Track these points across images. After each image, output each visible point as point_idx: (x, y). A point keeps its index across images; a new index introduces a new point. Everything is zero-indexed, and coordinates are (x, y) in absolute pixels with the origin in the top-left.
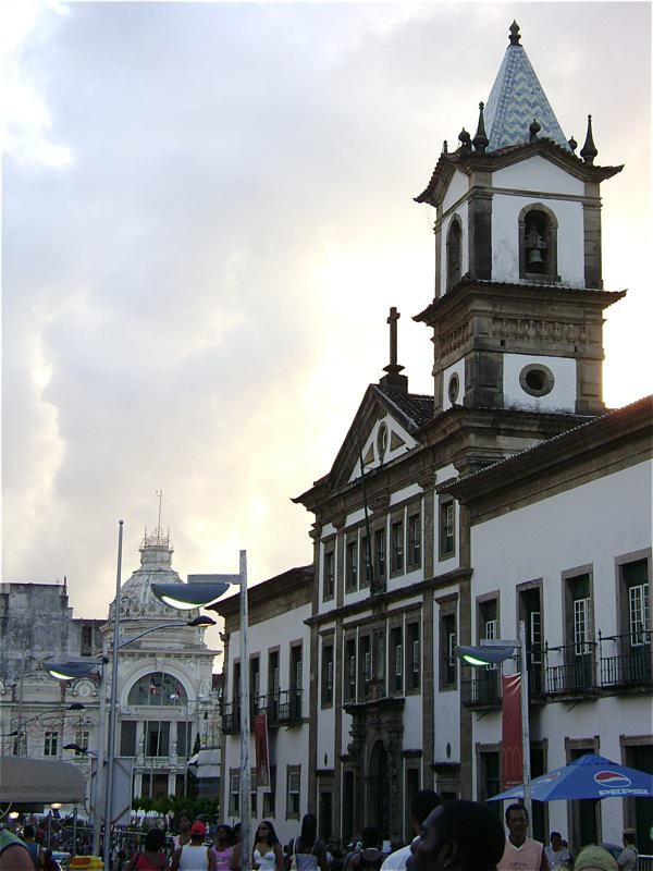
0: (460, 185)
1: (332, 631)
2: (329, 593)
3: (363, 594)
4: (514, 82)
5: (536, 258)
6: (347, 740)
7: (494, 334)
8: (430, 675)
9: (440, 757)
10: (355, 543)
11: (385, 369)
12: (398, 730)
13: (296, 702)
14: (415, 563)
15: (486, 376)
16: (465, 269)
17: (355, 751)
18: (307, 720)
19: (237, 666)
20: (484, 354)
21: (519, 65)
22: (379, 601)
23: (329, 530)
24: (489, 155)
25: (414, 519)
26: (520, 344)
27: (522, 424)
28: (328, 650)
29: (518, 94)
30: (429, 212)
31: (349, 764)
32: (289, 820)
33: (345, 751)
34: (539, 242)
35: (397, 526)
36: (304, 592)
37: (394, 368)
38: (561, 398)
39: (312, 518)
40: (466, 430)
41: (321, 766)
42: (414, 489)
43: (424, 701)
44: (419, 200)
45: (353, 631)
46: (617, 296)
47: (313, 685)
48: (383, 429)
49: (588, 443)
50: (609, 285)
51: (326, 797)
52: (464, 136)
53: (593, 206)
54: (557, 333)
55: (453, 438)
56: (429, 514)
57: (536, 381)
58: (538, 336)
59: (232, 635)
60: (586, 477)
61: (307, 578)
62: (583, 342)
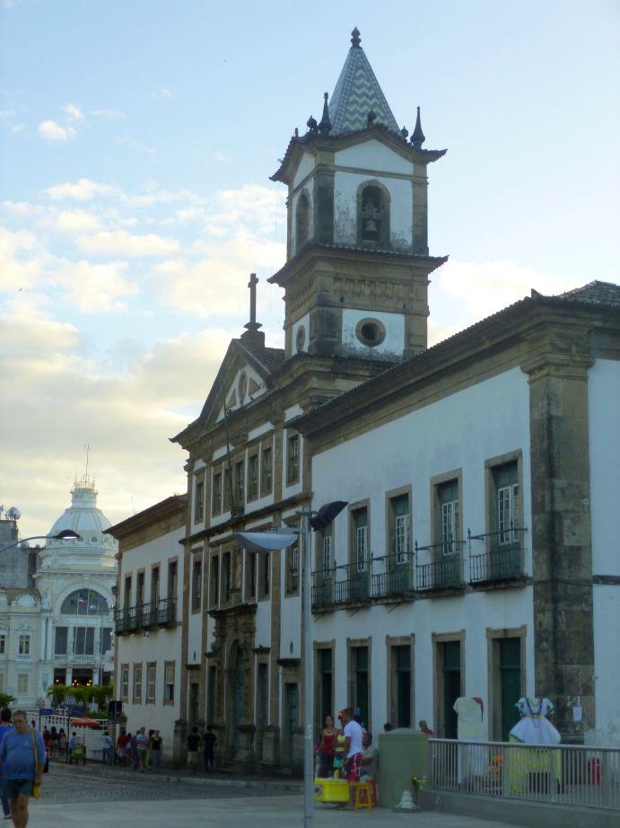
0: (308, 164)
1: (200, 549)
2: (199, 518)
3: (225, 517)
4: (355, 77)
5: (371, 227)
6: (211, 639)
7: (335, 292)
8: (277, 584)
9: (285, 654)
10: (219, 475)
11: (246, 326)
12: (251, 631)
13: (172, 608)
14: (267, 490)
15: (327, 325)
16: (311, 235)
17: (217, 651)
18: (180, 624)
19: (129, 580)
20: (326, 309)
21: (359, 64)
22: (239, 521)
23: (200, 464)
24: (332, 138)
25: (267, 452)
26: (357, 301)
27: (357, 369)
28: (198, 565)
29: (359, 88)
30: (282, 190)
31: (212, 660)
32: (166, 706)
33: (209, 650)
34: (375, 214)
35: (253, 458)
36: (180, 516)
37: (253, 326)
38: (393, 344)
39: (186, 454)
40: (308, 374)
41: (191, 661)
42: (267, 427)
44: (274, 178)
45: (217, 548)
46: (440, 261)
47: (186, 594)
48: (243, 377)
49: (409, 379)
50: (434, 252)
51: (195, 687)
52: (312, 123)
53: (420, 184)
54: (389, 292)
55: (299, 381)
56: (279, 447)
57: (370, 332)
58: (373, 294)
59: (124, 554)
60: (408, 409)
62: (410, 300)
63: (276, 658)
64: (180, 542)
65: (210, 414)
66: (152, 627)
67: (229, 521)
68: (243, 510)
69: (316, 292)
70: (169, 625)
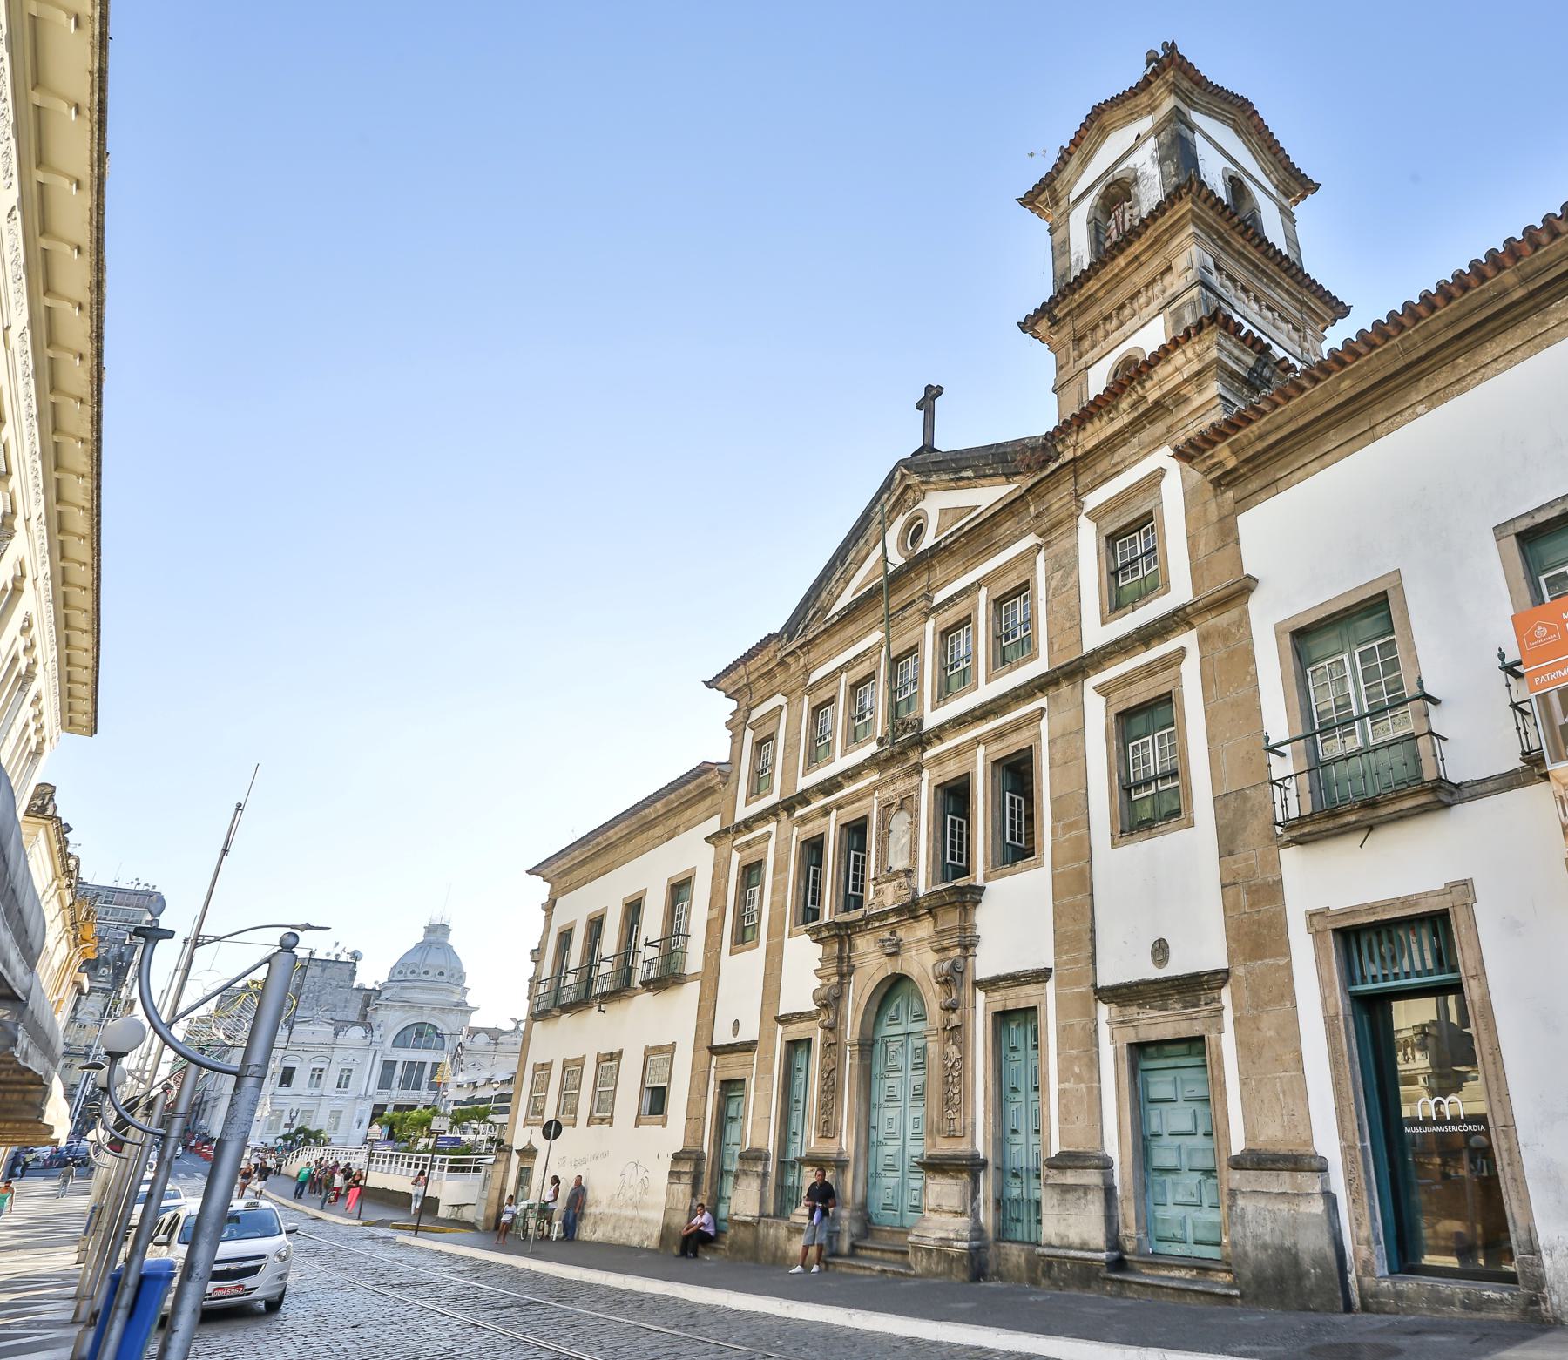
28: (752, 872)
39: (732, 705)
42: (1031, 540)
65: (811, 612)
66: (621, 990)
67: (874, 756)
68: (921, 722)
70: (667, 979)
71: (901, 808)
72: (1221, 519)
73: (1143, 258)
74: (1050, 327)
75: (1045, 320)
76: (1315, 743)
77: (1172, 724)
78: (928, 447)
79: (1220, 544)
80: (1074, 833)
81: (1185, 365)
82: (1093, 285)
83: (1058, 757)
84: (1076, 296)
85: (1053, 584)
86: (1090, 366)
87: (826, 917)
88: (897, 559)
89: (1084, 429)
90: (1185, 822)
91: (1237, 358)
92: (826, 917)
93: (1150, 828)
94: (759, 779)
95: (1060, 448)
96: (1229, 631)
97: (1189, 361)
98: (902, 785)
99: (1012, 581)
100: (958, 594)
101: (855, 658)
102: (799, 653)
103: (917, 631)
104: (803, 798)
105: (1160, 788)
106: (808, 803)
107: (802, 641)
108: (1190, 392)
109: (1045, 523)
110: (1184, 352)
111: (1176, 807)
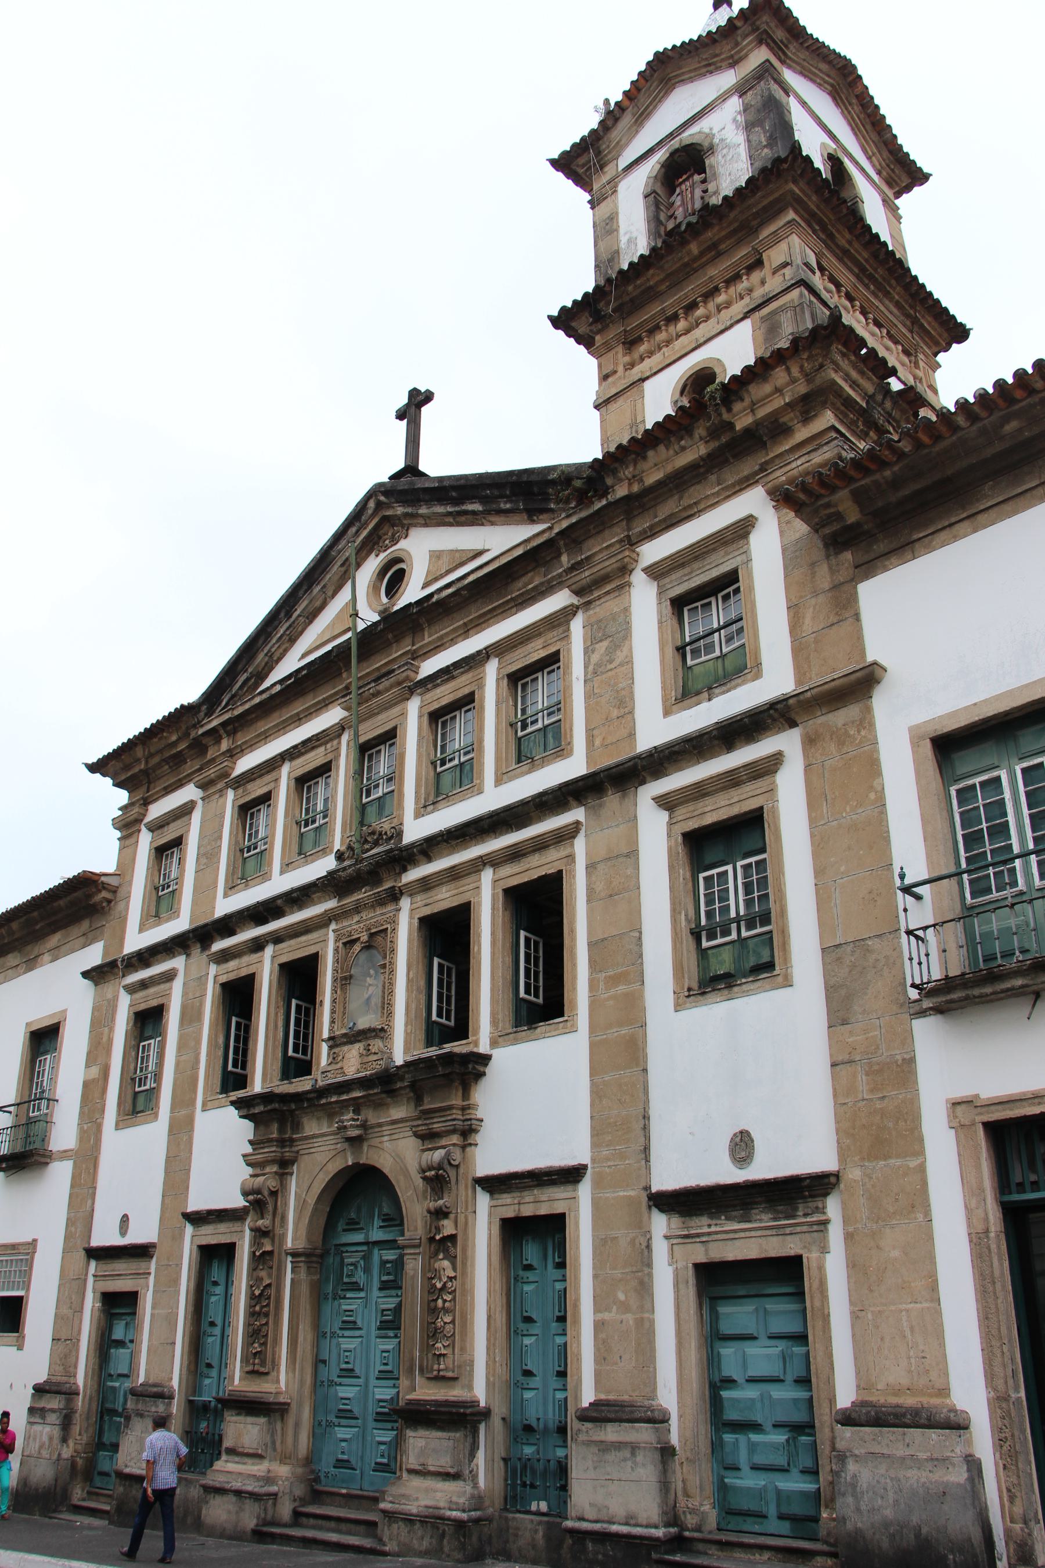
3: (323, 866)
18: (64, 1155)
39: (122, 796)
42: (559, 600)
43: (593, 1046)
61: (104, 894)
63: (634, 1192)
64: (86, 975)
67: (331, 874)
68: (400, 834)
69: (785, 265)
71: (368, 947)
72: (835, 587)
73: (723, 247)
74: (591, 324)
75: (587, 314)
76: (961, 884)
77: (763, 850)
78: (411, 469)
79: (833, 619)
80: (622, 988)
81: (788, 385)
82: (653, 275)
83: (599, 887)
84: (630, 288)
85: (595, 658)
86: (647, 378)
87: (257, 1086)
88: (369, 616)
89: (645, 458)
90: (780, 979)
91: (854, 382)
92: (257, 1086)
93: (730, 987)
94: (159, 898)
95: (609, 481)
96: (846, 731)
97: (793, 381)
98: (373, 917)
99: (535, 652)
100: (457, 665)
101: (304, 743)
102: (222, 732)
103: (395, 711)
104: (227, 925)
105: (745, 934)
106: (232, 933)
107: (226, 717)
108: (792, 420)
109: (586, 575)
110: (788, 369)
111: (765, 958)
